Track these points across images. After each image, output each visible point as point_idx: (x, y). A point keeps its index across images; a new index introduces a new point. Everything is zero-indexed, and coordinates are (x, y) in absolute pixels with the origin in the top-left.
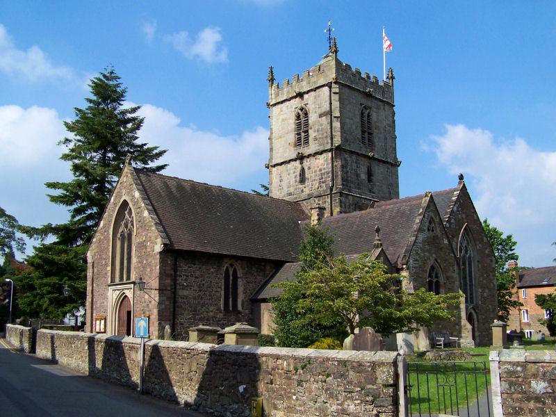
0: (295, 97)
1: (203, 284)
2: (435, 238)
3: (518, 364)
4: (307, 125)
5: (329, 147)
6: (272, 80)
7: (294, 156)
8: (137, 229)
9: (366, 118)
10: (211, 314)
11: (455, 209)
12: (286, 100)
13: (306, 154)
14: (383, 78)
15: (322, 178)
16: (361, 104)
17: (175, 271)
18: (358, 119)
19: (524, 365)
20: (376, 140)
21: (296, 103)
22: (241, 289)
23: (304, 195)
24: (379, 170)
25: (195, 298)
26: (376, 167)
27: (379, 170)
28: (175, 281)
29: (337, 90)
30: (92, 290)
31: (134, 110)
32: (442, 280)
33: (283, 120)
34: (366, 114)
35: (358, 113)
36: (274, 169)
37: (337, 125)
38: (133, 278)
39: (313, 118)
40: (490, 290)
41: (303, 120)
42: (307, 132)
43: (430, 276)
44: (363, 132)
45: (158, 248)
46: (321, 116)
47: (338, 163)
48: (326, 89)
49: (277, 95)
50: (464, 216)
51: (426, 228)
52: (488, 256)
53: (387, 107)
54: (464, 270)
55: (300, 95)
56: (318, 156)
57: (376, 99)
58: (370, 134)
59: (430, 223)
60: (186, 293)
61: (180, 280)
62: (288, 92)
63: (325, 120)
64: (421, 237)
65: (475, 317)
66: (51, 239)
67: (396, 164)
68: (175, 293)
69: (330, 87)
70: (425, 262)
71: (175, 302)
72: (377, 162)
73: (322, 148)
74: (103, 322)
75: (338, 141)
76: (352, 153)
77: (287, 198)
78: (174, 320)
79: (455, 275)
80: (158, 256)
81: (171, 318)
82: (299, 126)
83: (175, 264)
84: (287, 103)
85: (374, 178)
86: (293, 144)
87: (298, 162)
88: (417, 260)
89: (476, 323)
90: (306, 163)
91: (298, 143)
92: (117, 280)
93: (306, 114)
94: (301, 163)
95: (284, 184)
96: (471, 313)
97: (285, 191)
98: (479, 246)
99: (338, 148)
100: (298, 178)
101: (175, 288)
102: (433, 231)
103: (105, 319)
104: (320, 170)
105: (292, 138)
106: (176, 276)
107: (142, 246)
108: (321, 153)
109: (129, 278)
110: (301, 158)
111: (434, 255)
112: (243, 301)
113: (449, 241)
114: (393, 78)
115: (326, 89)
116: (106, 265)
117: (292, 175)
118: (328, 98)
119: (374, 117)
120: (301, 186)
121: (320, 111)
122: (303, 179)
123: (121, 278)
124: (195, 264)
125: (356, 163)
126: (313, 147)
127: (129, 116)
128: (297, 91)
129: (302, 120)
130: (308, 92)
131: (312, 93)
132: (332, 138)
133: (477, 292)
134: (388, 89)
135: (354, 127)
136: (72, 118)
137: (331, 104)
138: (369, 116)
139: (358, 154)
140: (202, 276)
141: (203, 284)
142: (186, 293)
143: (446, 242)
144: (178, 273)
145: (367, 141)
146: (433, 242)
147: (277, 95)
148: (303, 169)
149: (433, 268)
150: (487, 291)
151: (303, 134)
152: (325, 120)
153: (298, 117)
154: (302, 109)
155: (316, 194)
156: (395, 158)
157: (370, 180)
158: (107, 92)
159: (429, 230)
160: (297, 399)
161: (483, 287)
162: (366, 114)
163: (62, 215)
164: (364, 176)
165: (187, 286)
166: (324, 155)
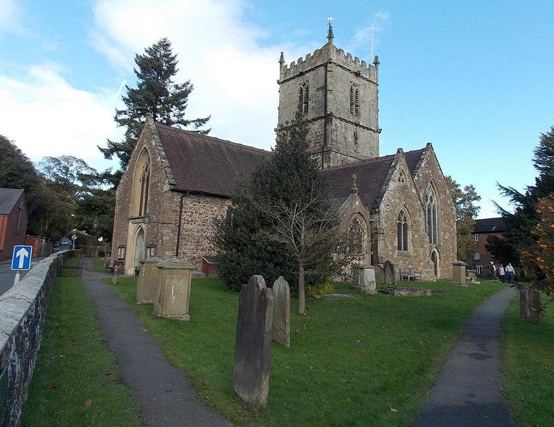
1: (207, 220)
2: (405, 188)
4: (307, 97)
5: (323, 115)
12: (293, 78)
15: (317, 140)
16: (351, 82)
17: (181, 208)
18: (348, 94)
21: (300, 80)
24: (363, 134)
25: (198, 232)
26: (361, 133)
27: (363, 134)
32: (409, 224)
34: (354, 91)
39: (312, 91)
40: (450, 233)
42: (307, 103)
44: (352, 104)
46: (318, 90)
48: (322, 68)
50: (430, 172)
53: (372, 86)
54: (429, 218)
55: (302, 74)
59: (401, 174)
60: (190, 227)
61: (184, 216)
62: (294, 72)
63: (321, 93)
65: (438, 255)
67: (379, 131)
68: (179, 227)
70: (395, 207)
71: (179, 235)
79: (421, 219)
82: (301, 98)
83: (181, 202)
88: (388, 205)
89: (438, 260)
98: (442, 196)
102: (403, 181)
104: (316, 133)
105: (295, 108)
106: (181, 212)
107: (155, 185)
108: (319, 118)
111: (403, 202)
113: (417, 192)
118: (323, 76)
119: (361, 92)
121: (317, 87)
124: (199, 203)
125: (345, 128)
128: (301, 70)
131: (312, 72)
132: (326, 108)
137: (326, 80)
140: (205, 213)
141: (207, 220)
142: (190, 227)
143: (414, 191)
145: (354, 112)
150: (448, 234)
156: (377, 126)
159: (399, 180)
161: (445, 231)
162: (354, 91)
164: (351, 139)
165: (192, 221)
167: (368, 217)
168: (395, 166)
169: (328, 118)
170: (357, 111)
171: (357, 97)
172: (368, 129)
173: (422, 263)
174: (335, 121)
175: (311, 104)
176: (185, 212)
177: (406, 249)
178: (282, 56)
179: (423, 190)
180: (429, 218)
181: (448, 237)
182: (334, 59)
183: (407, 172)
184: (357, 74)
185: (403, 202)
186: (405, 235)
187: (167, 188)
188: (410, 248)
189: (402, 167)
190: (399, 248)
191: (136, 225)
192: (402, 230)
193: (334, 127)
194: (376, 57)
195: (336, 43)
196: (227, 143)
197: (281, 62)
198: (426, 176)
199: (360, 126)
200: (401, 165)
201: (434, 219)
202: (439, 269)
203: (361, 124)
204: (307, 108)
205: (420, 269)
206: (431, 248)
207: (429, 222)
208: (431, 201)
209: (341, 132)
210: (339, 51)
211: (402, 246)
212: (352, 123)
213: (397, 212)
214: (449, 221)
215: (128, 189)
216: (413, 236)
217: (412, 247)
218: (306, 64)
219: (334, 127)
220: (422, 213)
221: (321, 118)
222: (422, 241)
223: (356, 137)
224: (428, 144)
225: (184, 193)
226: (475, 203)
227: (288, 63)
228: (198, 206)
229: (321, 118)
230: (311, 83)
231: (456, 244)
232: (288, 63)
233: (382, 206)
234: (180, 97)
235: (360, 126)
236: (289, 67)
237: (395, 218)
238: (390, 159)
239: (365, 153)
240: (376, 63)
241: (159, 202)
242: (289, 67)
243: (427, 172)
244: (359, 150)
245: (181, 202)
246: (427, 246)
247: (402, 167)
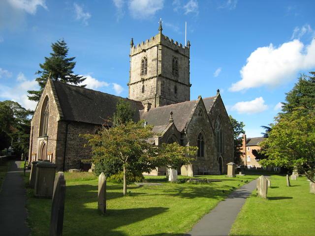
0: (142, 52)
4: (146, 65)
5: (156, 75)
6: (133, 44)
7: (140, 80)
10: (86, 154)
11: (214, 106)
13: (145, 79)
14: (185, 45)
16: (173, 56)
17: (67, 130)
20: (179, 73)
21: (143, 55)
23: (143, 98)
24: (180, 88)
25: (77, 145)
26: (179, 87)
27: (180, 88)
28: (66, 136)
29: (161, 48)
31: (71, 59)
32: (205, 140)
33: (136, 63)
35: (171, 60)
36: (131, 86)
37: (160, 65)
39: (149, 61)
41: (145, 62)
42: (146, 68)
43: (199, 138)
44: (173, 69)
45: (58, 119)
46: (153, 61)
47: (160, 83)
49: (134, 51)
50: (219, 110)
51: (198, 114)
52: (231, 130)
53: (186, 58)
55: (144, 51)
56: (150, 80)
57: (180, 53)
58: (176, 70)
59: (200, 111)
60: (72, 142)
61: (69, 136)
63: (155, 63)
64: (195, 118)
65: (222, 159)
67: (190, 85)
68: (66, 142)
69: (158, 47)
72: (179, 84)
73: (152, 76)
75: (160, 72)
76: (167, 78)
77: (136, 100)
79: (212, 138)
80: (57, 123)
81: (63, 155)
82: (143, 65)
83: (67, 128)
84: (138, 55)
85: (178, 91)
86: (140, 74)
87: (142, 82)
89: (223, 162)
90: (146, 83)
93: (146, 60)
94: (143, 83)
95: (135, 93)
96: (220, 158)
97: (136, 96)
98: (226, 125)
99: (160, 75)
100: (141, 90)
101: (66, 140)
103: (36, 155)
105: (139, 71)
106: (67, 134)
107: (52, 118)
110: (143, 80)
111: (201, 128)
114: (190, 45)
115: (156, 48)
116: (38, 128)
117: (139, 89)
119: (179, 62)
120: (142, 94)
126: (149, 75)
127: (69, 62)
129: (144, 62)
131: (149, 50)
133: (224, 147)
134: (187, 49)
135: (169, 66)
136: (43, 62)
138: (177, 62)
139: (170, 79)
142: (72, 142)
143: (208, 121)
144: (68, 132)
146: (201, 121)
147: (134, 51)
148: (144, 86)
149: (200, 134)
151: (145, 70)
153: (143, 61)
154: (145, 58)
155: (148, 98)
157: (176, 92)
158: (60, 50)
159: (199, 115)
161: (227, 145)
164: (172, 90)
166: (154, 79)
170: (176, 73)
173: (212, 164)
175: (148, 69)
176: (69, 134)
177: (203, 155)
179: (214, 121)
184: (177, 51)
185: (201, 128)
188: (206, 155)
199: (179, 82)
201: (221, 137)
203: (179, 81)
204: (146, 71)
205: (211, 167)
206: (218, 155)
208: (219, 128)
212: (173, 81)
213: (198, 134)
214: (230, 139)
216: (207, 148)
217: (206, 155)
220: (213, 134)
223: (176, 89)
231: (233, 153)
235: (179, 82)
237: (196, 138)
243: (217, 110)
244: (178, 97)
245: (67, 128)
246: (215, 154)
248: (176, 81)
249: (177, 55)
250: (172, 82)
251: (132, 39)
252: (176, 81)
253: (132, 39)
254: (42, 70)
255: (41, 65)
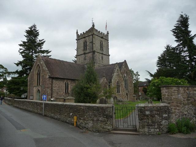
0: (83, 38)
2: (119, 74)
3: (143, 107)
4: (86, 45)
7: (83, 53)
8: (42, 72)
9: (101, 44)
12: (82, 39)
14: (106, 33)
17: (52, 83)
19: (144, 107)
21: (83, 39)
22: (69, 88)
27: (104, 57)
30: (29, 88)
32: (120, 85)
38: (41, 85)
39: (88, 43)
43: (117, 84)
46: (90, 43)
52: (132, 79)
55: (84, 37)
60: (55, 88)
61: (53, 85)
66: (16, 75)
67: (109, 55)
68: (52, 88)
74: (32, 96)
76: (98, 52)
78: (52, 95)
79: (123, 84)
85: (103, 59)
90: (86, 55)
91: (84, 50)
92: (36, 85)
93: (86, 42)
103: (33, 96)
105: (82, 48)
108: (90, 52)
109: (39, 85)
112: (70, 91)
115: (91, 36)
116: (33, 81)
122: (85, 59)
123: (37, 85)
128: (84, 36)
130: (87, 37)
131: (88, 37)
132: (93, 49)
137: (93, 40)
139: (99, 53)
142: (55, 88)
143: (121, 75)
149: (118, 82)
152: (91, 44)
153: (84, 43)
154: (85, 41)
157: (102, 60)
160: (86, 117)
163: (20, 68)
164: (101, 59)
167: (108, 84)
168: (116, 68)
169: (94, 52)
171: (102, 45)
172: (106, 55)
174: (96, 53)
177: (119, 92)
178: (77, 31)
180: (126, 84)
181: (131, 88)
182: (95, 33)
183: (119, 70)
184: (102, 38)
186: (119, 88)
187: (48, 77)
189: (118, 68)
190: (117, 92)
191: (36, 89)
192: (118, 87)
193: (95, 55)
194: (108, 32)
195: (95, 27)
196: (63, 61)
197: (77, 33)
198: (124, 70)
200: (117, 68)
201: (127, 83)
202: (129, 98)
204: (86, 49)
207: (126, 84)
209: (98, 56)
210: (97, 30)
211: (118, 92)
212: (101, 53)
213: (117, 82)
215: (32, 78)
218: (86, 34)
219: (95, 55)
221: (92, 52)
222: (124, 90)
224: (125, 61)
225: (53, 78)
226: (139, 77)
227: (79, 33)
228: (57, 82)
229: (92, 52)
230: (87, 40)
231: (133, 90)
232: (79, 33)
233: (113, 80)
234: (41, 44)
236: (80, 35)
237: (116, 84)
238: (113, 65)
239: (105, 63)
240: (108, 33)
241: (45, 81)
242: (80, 35)
247: (118, 68)
248: (102, 54)
249: (102, 40)
250: (100, 54)
251: (77, 30)
252: (102, 54)
253: (77, 30)
254: (21, 47)
255: (21, 45)
